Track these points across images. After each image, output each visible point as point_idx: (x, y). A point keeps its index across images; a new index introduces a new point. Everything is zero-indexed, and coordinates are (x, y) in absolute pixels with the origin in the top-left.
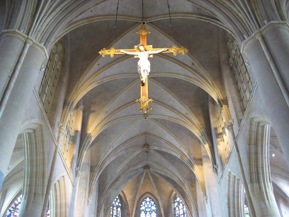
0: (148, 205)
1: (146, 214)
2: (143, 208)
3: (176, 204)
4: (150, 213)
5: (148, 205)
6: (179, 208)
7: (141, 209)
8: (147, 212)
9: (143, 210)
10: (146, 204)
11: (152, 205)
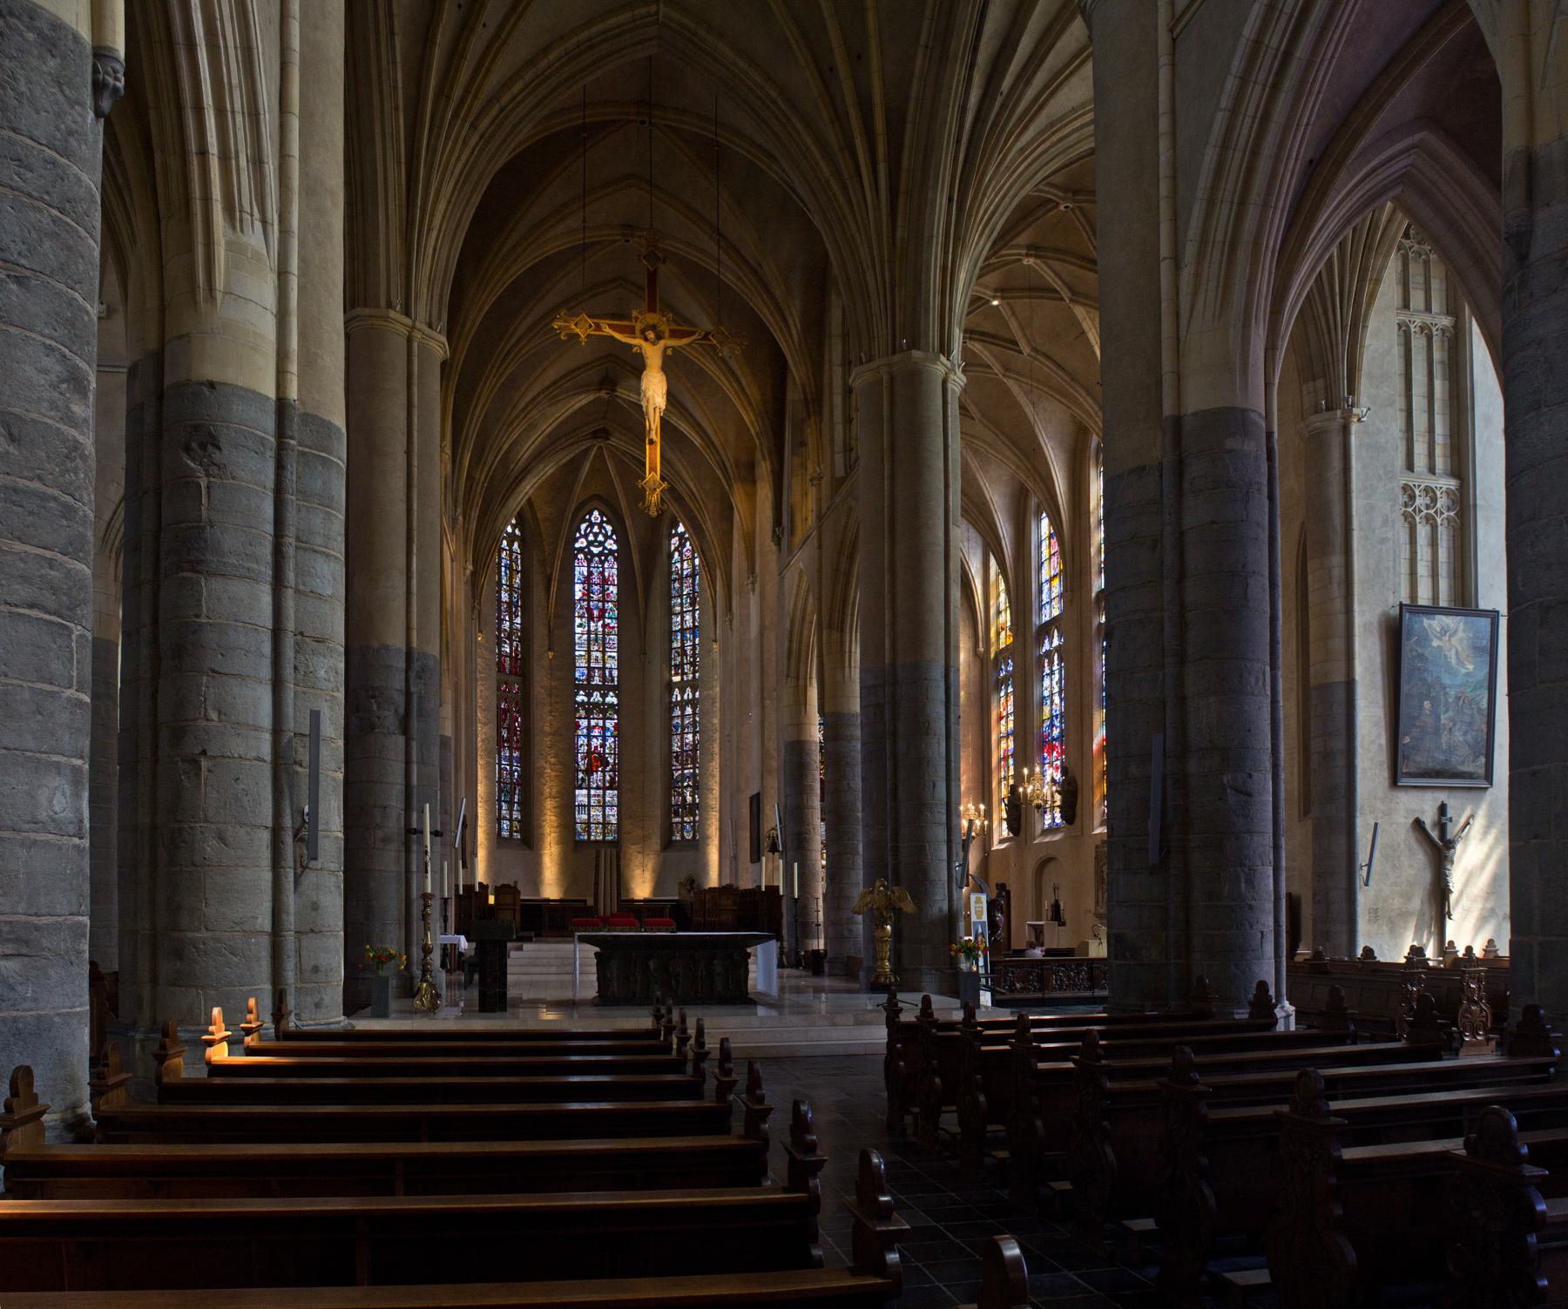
0: (596, 535)
1: (589, 562)
2: (581, 543)
3: (675, 541)
4: (600, 559)
5: (596, 535)
6: (681, 554)
7: (577, 545)
8: (593, 555)
9: (581, 550)
10: (591, 531)
11: (607, 537)
